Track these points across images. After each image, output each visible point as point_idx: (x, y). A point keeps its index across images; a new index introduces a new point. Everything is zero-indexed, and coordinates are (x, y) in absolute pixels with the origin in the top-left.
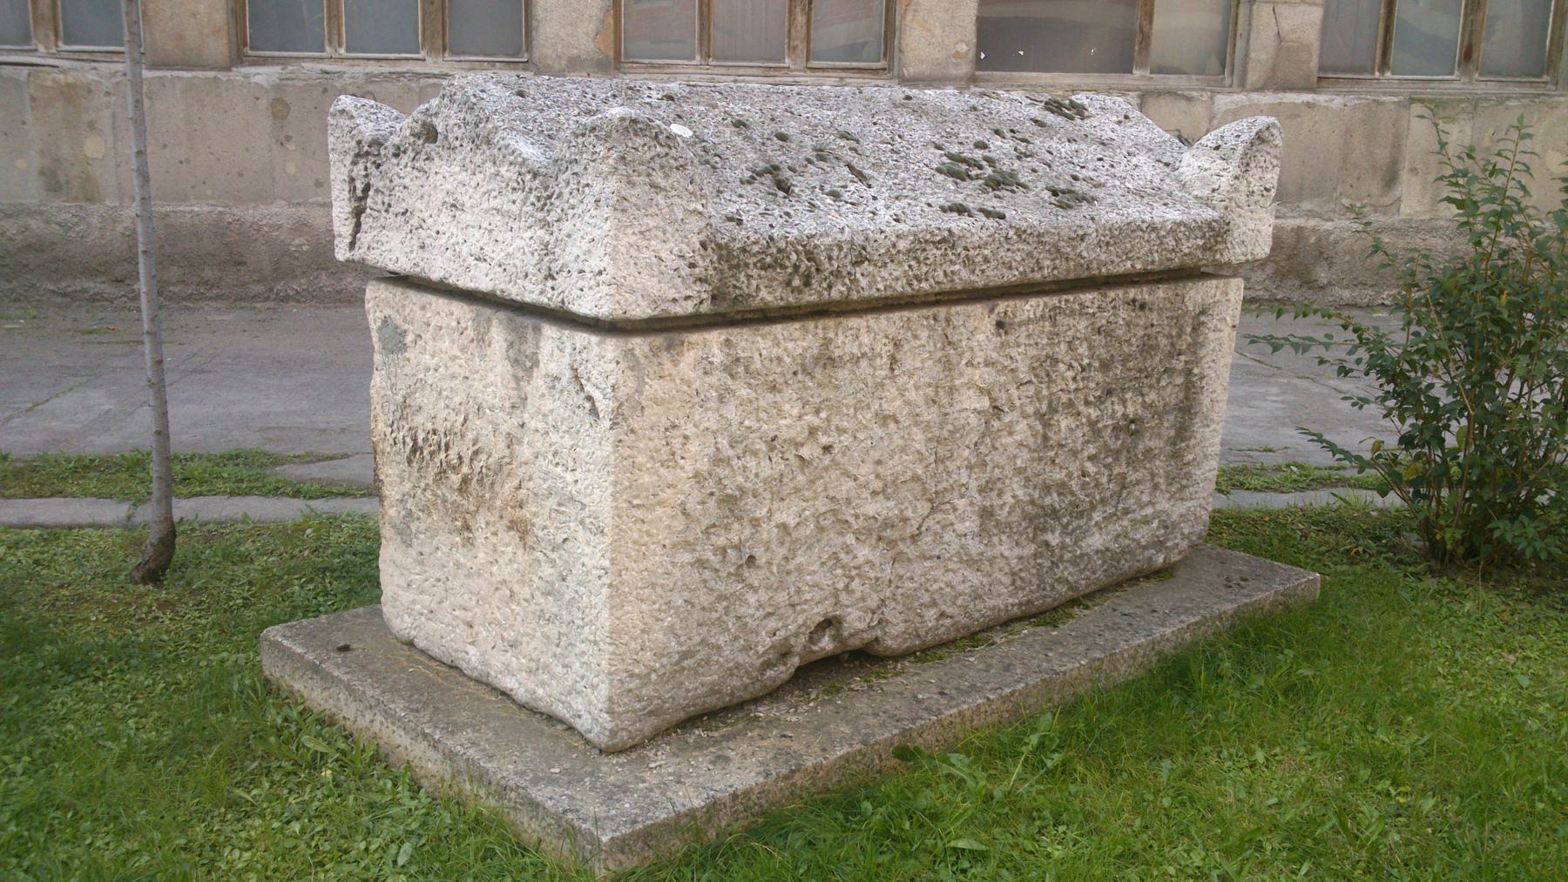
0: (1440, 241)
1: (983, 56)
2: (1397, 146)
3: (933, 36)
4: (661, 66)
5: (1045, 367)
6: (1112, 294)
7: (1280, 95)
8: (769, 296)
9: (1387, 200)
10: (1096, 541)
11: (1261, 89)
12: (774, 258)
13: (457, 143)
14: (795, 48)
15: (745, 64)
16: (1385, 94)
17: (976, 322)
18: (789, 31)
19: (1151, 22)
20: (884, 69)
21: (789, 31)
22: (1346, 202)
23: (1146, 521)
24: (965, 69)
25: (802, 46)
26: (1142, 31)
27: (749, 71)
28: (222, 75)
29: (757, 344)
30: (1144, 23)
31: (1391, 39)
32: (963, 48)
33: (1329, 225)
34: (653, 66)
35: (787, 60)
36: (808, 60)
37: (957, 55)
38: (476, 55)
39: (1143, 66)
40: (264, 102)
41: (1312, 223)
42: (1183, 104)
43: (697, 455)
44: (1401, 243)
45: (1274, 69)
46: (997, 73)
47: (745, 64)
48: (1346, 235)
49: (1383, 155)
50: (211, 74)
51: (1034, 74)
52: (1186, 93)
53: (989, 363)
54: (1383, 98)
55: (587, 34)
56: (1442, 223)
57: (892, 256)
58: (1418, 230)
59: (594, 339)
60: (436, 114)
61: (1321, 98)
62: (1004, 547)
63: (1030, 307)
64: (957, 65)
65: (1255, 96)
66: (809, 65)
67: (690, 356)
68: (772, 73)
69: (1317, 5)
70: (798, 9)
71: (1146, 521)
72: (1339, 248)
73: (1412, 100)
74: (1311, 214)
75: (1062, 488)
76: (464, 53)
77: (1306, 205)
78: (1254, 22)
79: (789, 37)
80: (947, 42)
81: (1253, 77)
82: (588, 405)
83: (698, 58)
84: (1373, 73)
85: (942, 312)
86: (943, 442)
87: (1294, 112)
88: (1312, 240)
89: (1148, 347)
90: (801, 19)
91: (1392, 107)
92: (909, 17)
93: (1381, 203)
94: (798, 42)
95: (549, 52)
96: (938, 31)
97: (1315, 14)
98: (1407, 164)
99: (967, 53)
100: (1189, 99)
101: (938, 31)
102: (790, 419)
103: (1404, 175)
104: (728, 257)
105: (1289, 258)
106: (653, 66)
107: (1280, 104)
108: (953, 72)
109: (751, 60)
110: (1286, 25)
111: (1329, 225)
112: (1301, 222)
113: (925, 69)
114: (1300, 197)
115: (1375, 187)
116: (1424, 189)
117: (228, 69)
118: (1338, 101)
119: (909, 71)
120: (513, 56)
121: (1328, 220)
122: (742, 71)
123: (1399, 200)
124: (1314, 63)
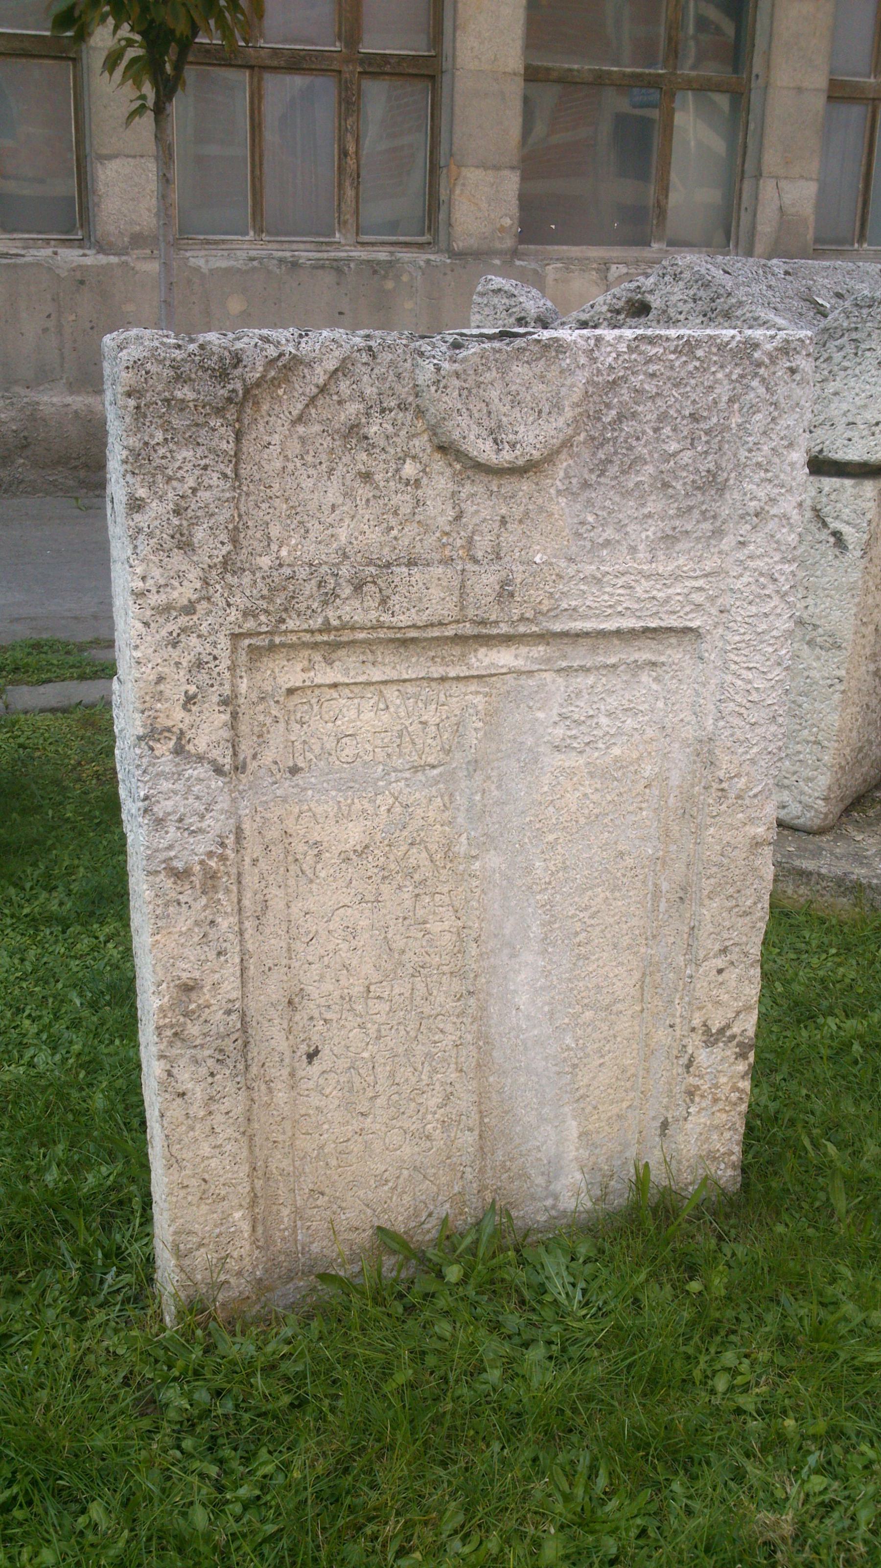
3: (480, 209)
4: (216, 242)
13: (682, 317)
14: (346, 222)
15: (305, 239)
18: (339, 205)
19: (667, 196)
20: (429, 243)
21: (339, 205)
24: (509, 243)
25: (351, 221)
26: (659, 206)
27: (302, 246)
30: (661, 197)
32: (507, 222)
34: (208, 242)
35: (337, 235)
36: (357, 234)
37: (502, 229)
38: (29, 232)
39: (659, 240)
46: (532, 247)
47: (305, 239)
51: (565, 248)
55: (149, 210)
59: (848, 482)
60: (651, 292)
64: (502, 238)
66: (360, 240)
68: (324, 248)
69: (811, 179)
70: (347, 183)
76: (15, 230)
78: (761, 196)
79: (339, 212)
80: (492, 216)
82: (832, 540)
83: (252, 233)
84: (853, 245)
90: (350, 193)
92: (457, 192)
94: (348, 217)
95: (112, 228)
96: (484, 205)
97: (810, 189)
99: (511, 227)
106: (208, 242)
108: (498, 245)
109: (304, 236)
110: (787, 199)
113: (472, 243)
119: (458, 245)
120: (67, 232)
122: (294, 246)
124: (810, 236)
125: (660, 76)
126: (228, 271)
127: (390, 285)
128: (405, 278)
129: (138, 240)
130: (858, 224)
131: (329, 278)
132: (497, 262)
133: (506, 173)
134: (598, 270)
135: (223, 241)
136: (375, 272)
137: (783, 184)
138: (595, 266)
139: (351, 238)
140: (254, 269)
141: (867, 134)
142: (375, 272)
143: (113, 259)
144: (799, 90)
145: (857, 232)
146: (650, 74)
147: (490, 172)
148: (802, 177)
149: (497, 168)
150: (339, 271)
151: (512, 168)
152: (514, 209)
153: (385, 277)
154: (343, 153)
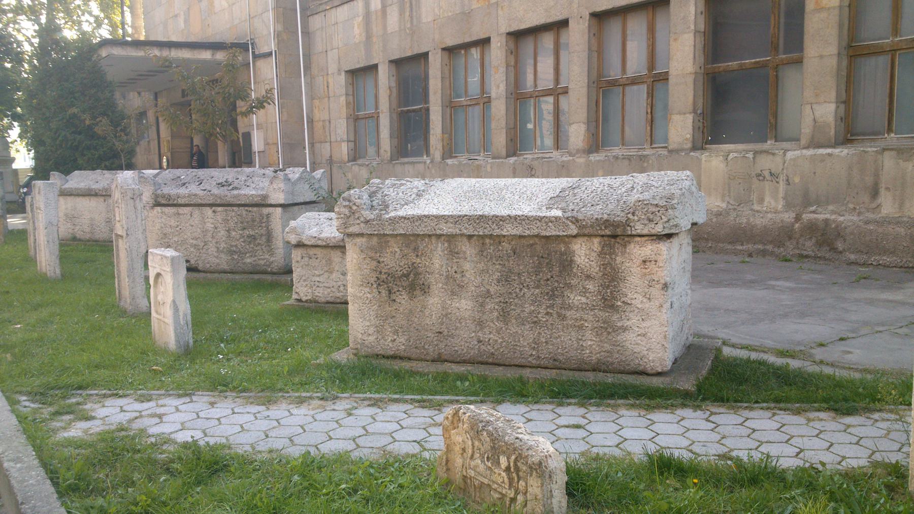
0: (903, 230)
1: (710, 138)
2: (877, 175)
3: (678, 132)
5: (226, 221)
6: (241, 208)
7: (816, 150)
8: (163, 202)
9: (874, 205)
10: (248, 260)
11: (807, 147)
12: (163, 196)
16: (871, 147)
17: (208, 211)
22: (851, 206)
23: (263, 259)
27: (633, 150)
28: (504, 160)
29: (166, 210)
31: (892, 115)
33: (842, 219)
37: (687, 139)
39: (771, 139)
40: (511, 168)
41: (833, 217)
42: (771, 157)
43: (158, 226)
44: (880, 230)
45: (813, 137)
48: (850, 224)
49: (869, 180)
50: (500, 160)
51: (728, 145)
52: (773, 152)
53: (212, 218)
54: (869, 149)
56: (905, 219)
57: (185, 197)
58: (889, 223)
61: (837, 151)
62: (223, 256)
63: (220, 209)
64: (686, 144)
65: (804, 151)
66: (652, 146)
67: (155, 210)
71: (263, 259)
72: (847, 231)
73: (884, 150)
74: (833, 212)
75: (236, 246)
77: (831, 208)
81: (803, 142)
85: (201, 208)
86: (204, 232)
87: (822, 159)
88: (833, 226)
89: (253, 221)
90: (649, 128)
91: (873, 154)
93: (870, 207)
96: (680, 130)
98: (883, 185)
100: (774, 154)
101: (680, 130)
102: (173, 222)
103: (882, 191)
104: (157, 196)
105: (822, 235)
107: (815, 155)
110: (818, 114)
111: (842, 219)
112: (828, 216)
114: (828, 204)
115: (866, 199)
116: (894, 199)
117: (506, 158)
118: (846, 151)
119: (670, 147)
121: (842, 216)
123: (879, 206)
125: (768, 60)
126: (599, 161)
127: (645, 164)
128: (650, 162)
129: (578, 151)
130: (886, 123)
131: (626, 162)
132: (683, 154)
133: (688, 115)
134: (723, 156)
135: (611, 150)
136: (641, 160)
137: (814, 106)
138: (722, 154)
139: (649, 146)
140: (606, 160)
141: (889, 71)
142: (641, 160)
143: (571, 158)
144: (821, 57)
145: (886, 128)
146: (763, 61)
147: (682, 116)
148: (825, 102)
149: (685, 114)
150: (629, 160)
151: (690, 113)
152: (691, 131)
153: (644, 162)
154: (647, 113)
